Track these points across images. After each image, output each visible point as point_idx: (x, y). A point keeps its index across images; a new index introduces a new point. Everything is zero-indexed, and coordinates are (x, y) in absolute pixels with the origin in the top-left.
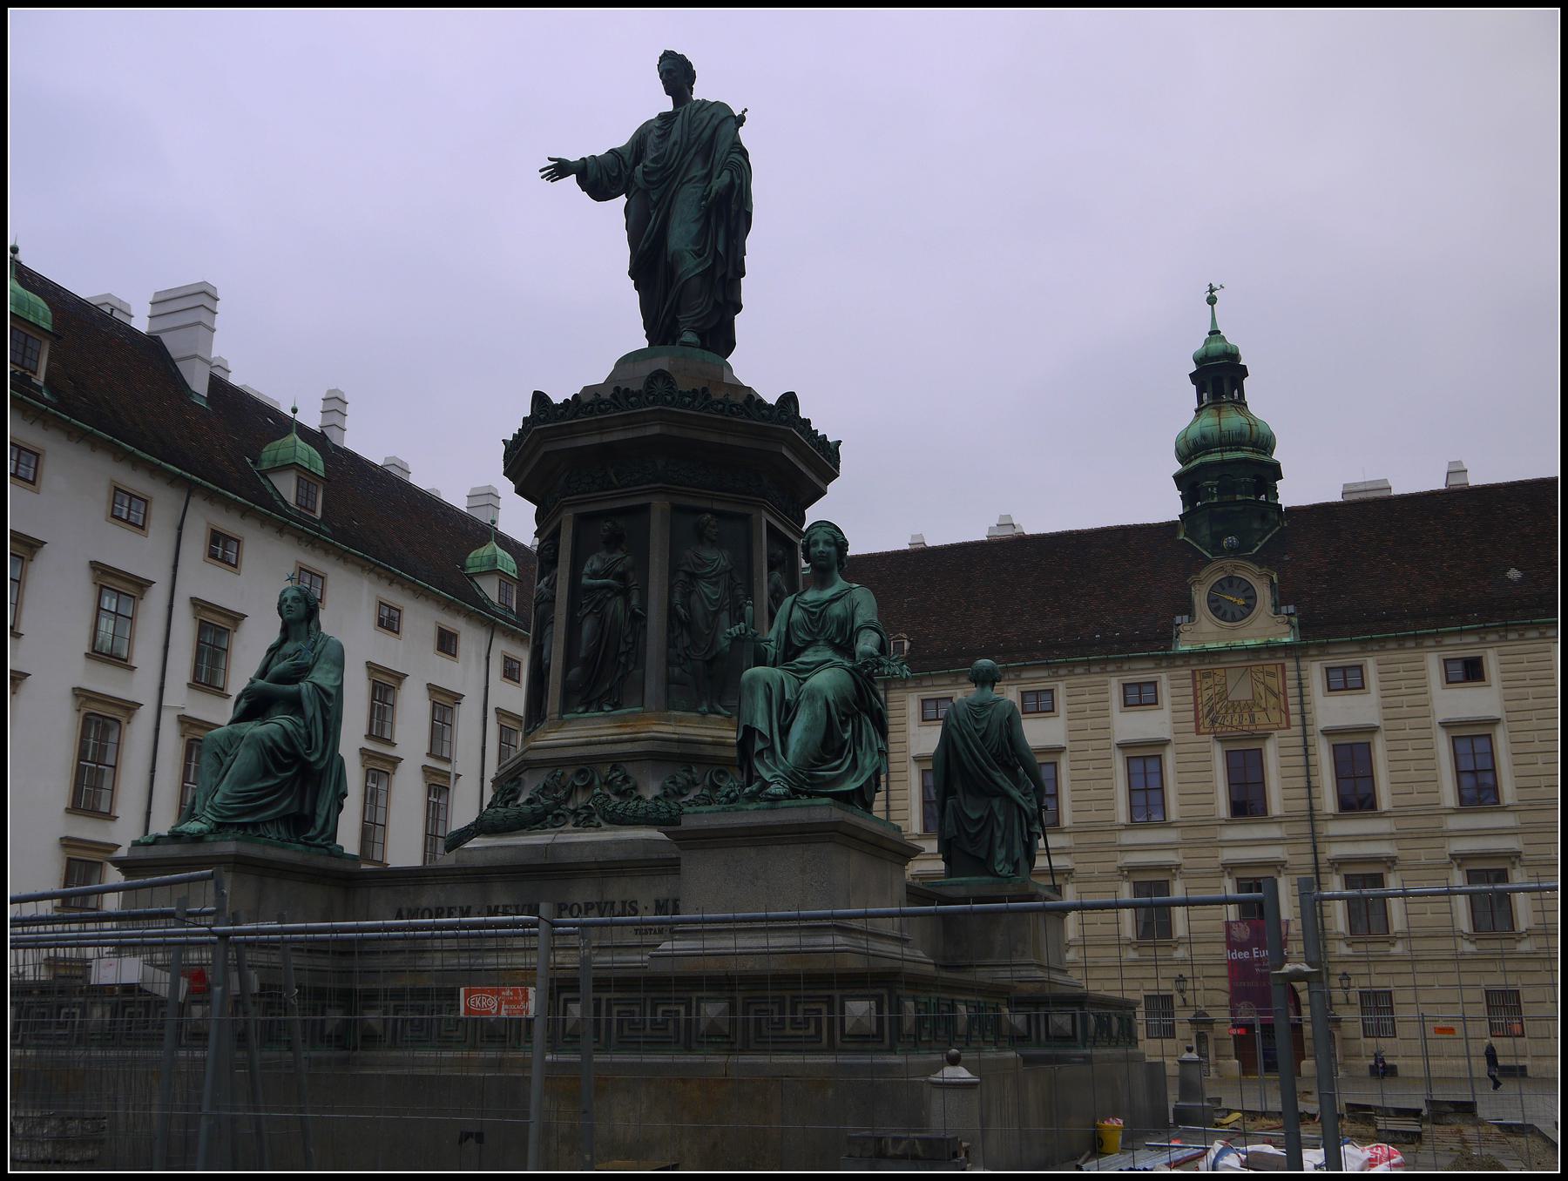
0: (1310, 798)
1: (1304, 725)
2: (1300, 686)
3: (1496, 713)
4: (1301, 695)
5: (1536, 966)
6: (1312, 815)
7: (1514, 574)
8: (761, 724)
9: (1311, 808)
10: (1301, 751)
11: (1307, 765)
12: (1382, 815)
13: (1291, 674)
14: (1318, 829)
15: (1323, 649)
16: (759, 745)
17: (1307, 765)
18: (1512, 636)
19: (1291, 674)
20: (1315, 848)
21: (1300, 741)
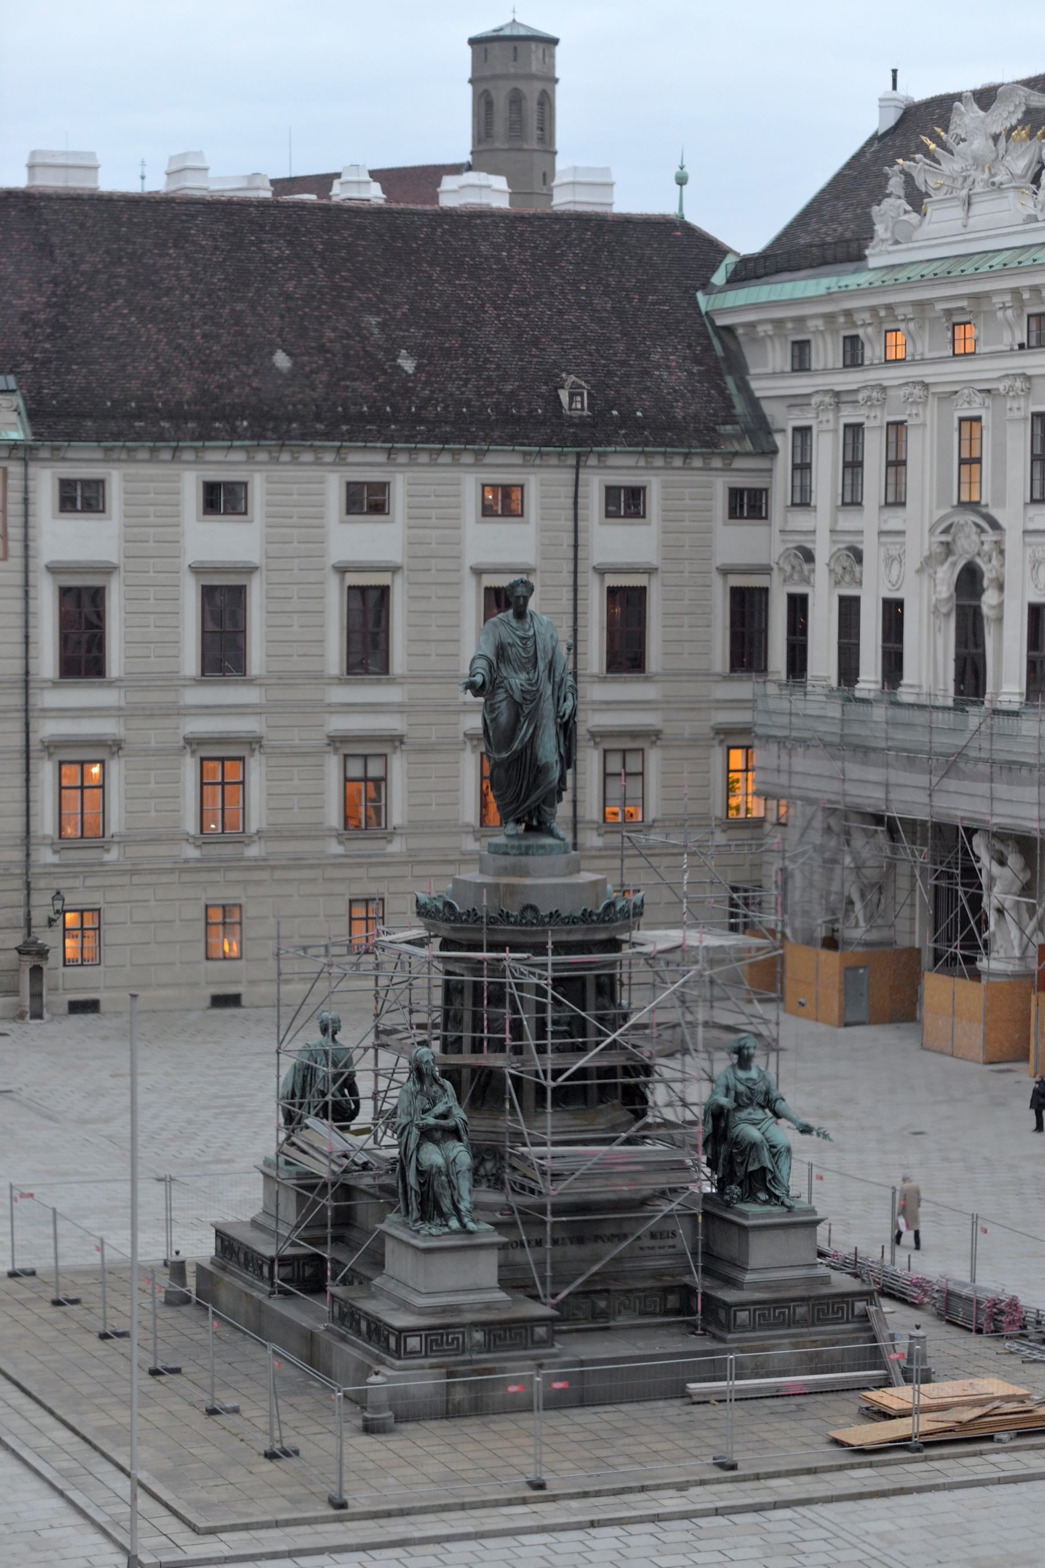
0: (27, 658)
1: (26, 557)
2: (26, 501)
3: (254, 557)
4: (26, 515)
5: (265, 875)
6: (27, 682)
7: (282, 360)
8: (770, 1166)
9: (27, 673)
10: (19, 593)
11: (27, 612)
12: (111, 684)
13: (15, 482)
14: (32, 701)
15: (57, 456)
16: (769, 1176)
17: (27, 612)
18: (285, 457)
19: (15, 482)
20: (27, 725)
21: (18, 579)
